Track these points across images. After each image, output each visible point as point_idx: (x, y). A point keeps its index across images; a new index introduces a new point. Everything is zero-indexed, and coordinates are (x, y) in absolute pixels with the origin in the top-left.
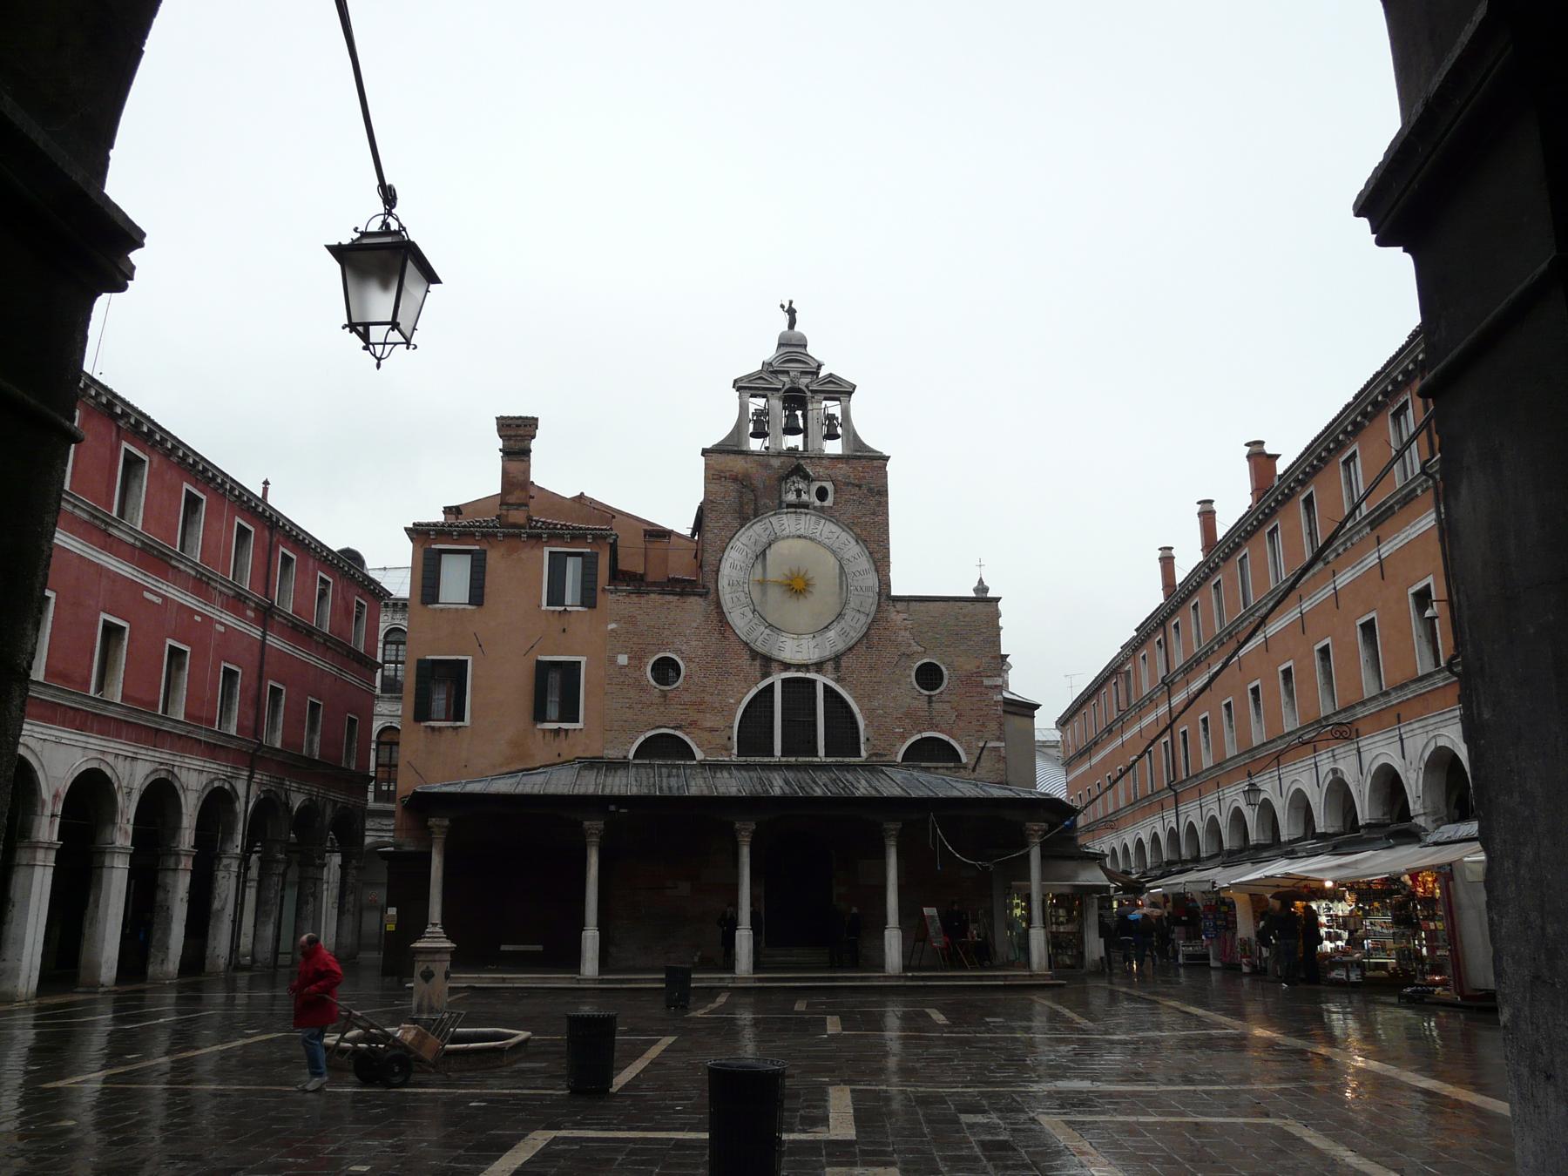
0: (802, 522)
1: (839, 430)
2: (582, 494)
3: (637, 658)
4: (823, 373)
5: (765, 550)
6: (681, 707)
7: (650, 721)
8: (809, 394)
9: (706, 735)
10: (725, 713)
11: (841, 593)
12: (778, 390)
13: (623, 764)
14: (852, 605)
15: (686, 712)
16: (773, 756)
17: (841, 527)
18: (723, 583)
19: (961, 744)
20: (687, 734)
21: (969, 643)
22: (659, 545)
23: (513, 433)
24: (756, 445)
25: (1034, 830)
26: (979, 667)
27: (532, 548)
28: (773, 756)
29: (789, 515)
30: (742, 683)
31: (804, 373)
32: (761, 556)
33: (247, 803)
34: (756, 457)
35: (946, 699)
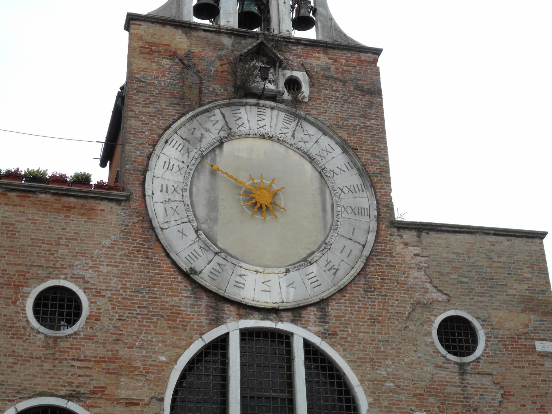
5: (213, 150)
6: (78, 364)
7: (26, 384)
10: (152, 377)
11: (324, 217)
14: (341, 230)
17: (320, 129)
26: (527, 326)
29: (248, 107)
34: (203, 34)
35: (487, 371)
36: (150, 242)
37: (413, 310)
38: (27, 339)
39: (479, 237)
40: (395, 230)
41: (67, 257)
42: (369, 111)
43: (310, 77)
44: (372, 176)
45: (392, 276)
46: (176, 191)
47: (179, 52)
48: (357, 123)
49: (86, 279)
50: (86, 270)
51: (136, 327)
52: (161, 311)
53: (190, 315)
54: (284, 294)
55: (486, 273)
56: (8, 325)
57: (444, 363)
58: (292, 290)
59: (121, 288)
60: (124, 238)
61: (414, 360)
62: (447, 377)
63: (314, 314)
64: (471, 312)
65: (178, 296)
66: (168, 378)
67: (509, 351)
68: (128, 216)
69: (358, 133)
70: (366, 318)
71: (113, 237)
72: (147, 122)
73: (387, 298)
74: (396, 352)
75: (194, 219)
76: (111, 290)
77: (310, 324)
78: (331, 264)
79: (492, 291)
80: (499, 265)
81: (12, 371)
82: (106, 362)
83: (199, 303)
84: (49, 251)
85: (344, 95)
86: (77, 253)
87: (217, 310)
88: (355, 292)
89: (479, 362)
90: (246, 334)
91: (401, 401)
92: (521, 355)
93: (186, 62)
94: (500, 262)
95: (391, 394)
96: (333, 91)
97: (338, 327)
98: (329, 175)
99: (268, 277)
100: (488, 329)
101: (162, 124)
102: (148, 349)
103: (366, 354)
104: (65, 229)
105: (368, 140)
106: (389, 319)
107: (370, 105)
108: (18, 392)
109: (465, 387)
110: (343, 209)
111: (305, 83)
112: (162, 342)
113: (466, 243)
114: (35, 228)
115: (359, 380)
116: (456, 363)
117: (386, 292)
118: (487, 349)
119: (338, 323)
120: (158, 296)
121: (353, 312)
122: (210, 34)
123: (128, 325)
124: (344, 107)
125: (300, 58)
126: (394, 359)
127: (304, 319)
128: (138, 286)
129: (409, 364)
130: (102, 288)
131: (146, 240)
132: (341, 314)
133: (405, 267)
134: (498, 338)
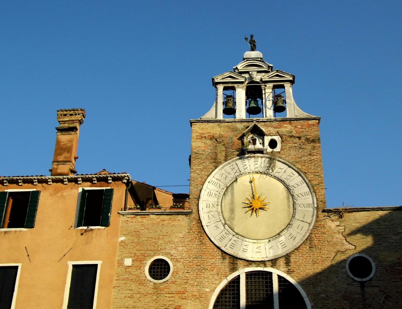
0: (259, 163)
3: (139, 260)
12: (242, 83)
15: (172, 299)
17: (287, 165)
18: (202, 205)
23: (67, 119)
30: (216, 276)
31: (258, 72)
34: (227, 124)
36: (202, 233)
37: (336, 255)
38: (146, 285)
41: (163, 245)
42: (313, 151)
43: (282, 138)
44: (314, 186)
45: (324, 238)
46: (214, 206)
47: (215, 136)
48: (306, 159)
49: (171, 254)
50: (171, 250)
51: (195, 275)
52: (207, 267)
53: (220, 268)
54: (268, 252)
55: (376, 232)
56: (137, 279)
57: (352, 282)
58: (271, 250)
59: (188, 257)
60: (189, 233)
61: (336, 282)
62: (354, 289)
63: (283, 262)
64: (368, 254)
65: (215, 259)
66: (210, 299)
67: (389, 273)
68: (191, 221)
69: (307, 164)
70: (310, 261)
71: (184, 233)
72: (199, 173)
73: (321, 250)
74: (326, 278)
75: (223, 219)
76: (183, 259)
77: (281, 267)
78: (292, 235)
79: (379, 241)
80: (384, 227)
81: (139, 301)
82: (181, 294)
83: (225, 261)
84: (155, 242)
85: (300, 145)
86: (167, 242)
87: (234, 264)
88: (304, 249)
89: (372, 281)
90: (249, 275)
92: (396, 275)
93: (218, 140)
94: (385, 225)
95: (323, 301)
96: (294, 143)
97: (295, 268)
98: (291, 188)
99: (259, 245)
100: (377, 262)
101: (207, 173)
102: (200, 286)
103: (310, 280)
104: (162, 231)
105: (312, 167)
106: (322, 261)
107: (314, 148)
109: (364, 294)
110: (299, 206)
111: (279, 142)
112: (207, 282)
113: (365, 217)
114: (148, 232)
115: (307, 294)
116: (359, 282)
117: (321, 247)
118: (377, 273)
119: (295, 265)
120: (205, 259)
121: (303, 259)
122: (230, 124)
123: (191, 275)
124: (299, 151)
125: (277, 129)
126: (325, 282)
127: (277, 265)
128: (196, 255)
129: (333, 284)
130: (179, 258)
131: (200, 232)
132: (297, 261)
133: (331, 233)
134: (382, 266)
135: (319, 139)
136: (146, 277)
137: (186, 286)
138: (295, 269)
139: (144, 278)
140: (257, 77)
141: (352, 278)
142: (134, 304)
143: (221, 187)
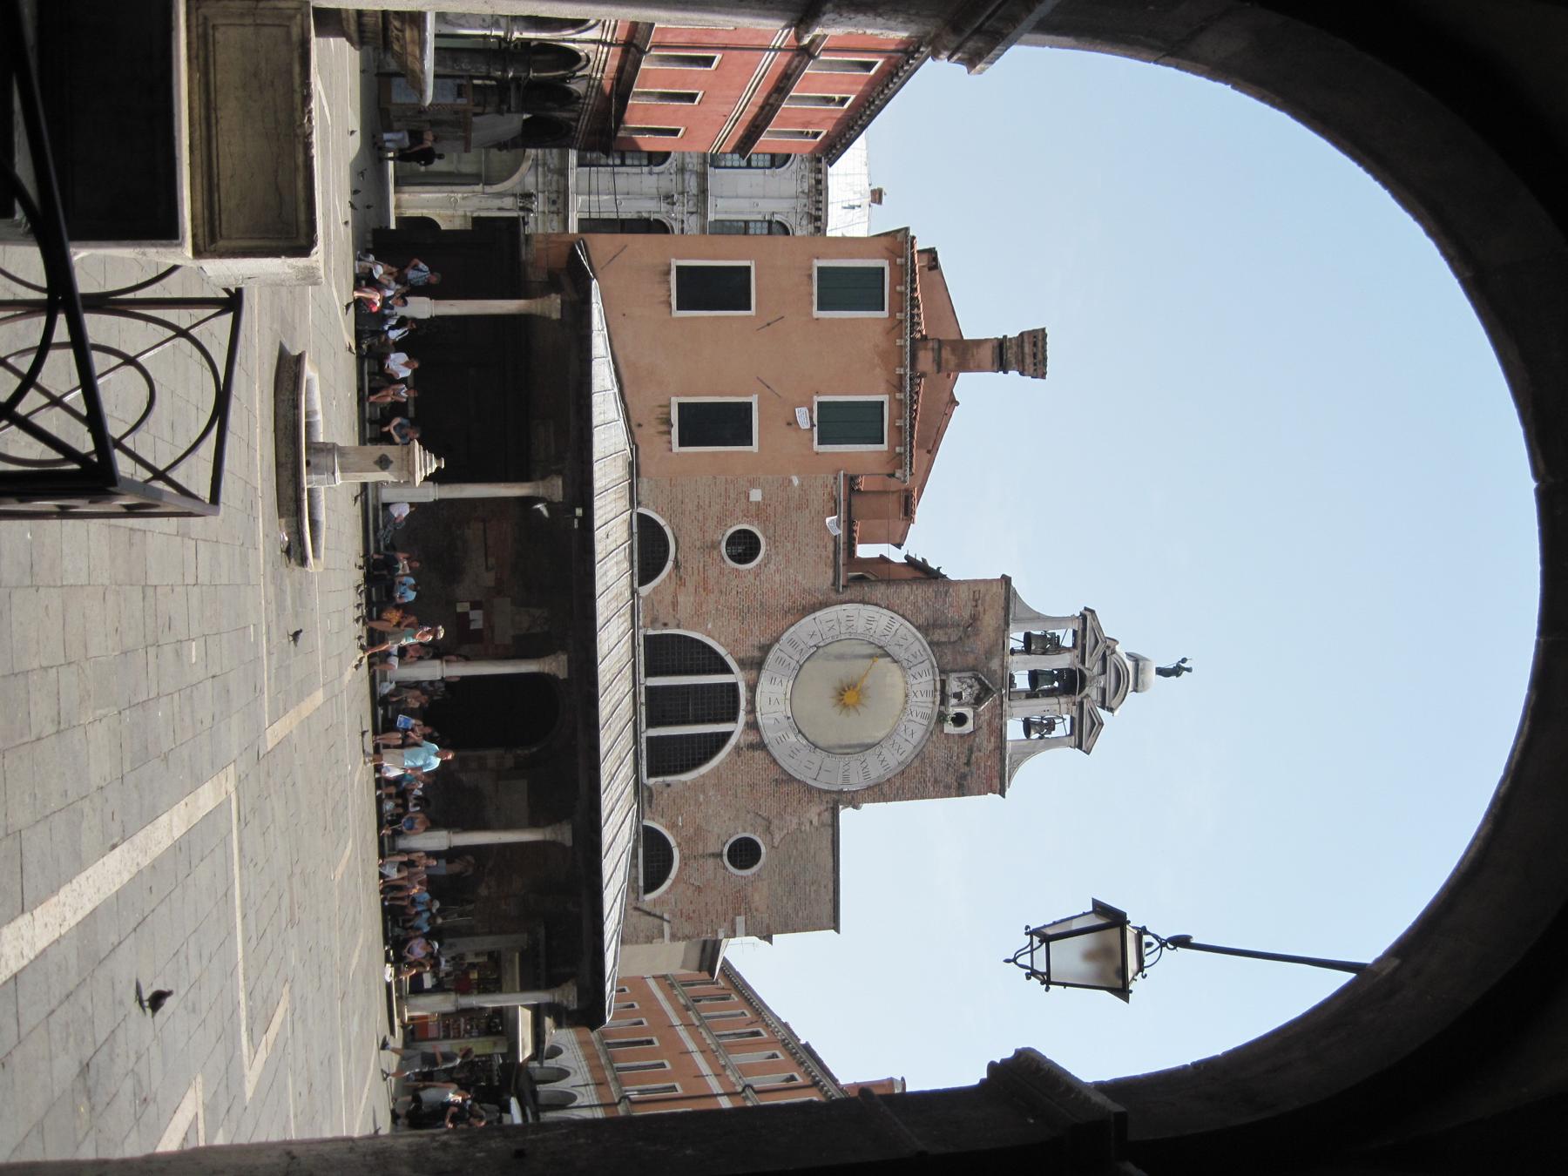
0: (924, 699)
1: (1035, 736)
2: (957, 404)
3: (759, 512)
4: (1103, 713)
5: (889, 655)
6: (701, 565)
8: (1078, 698)
9: (668, 599)
10: (695, 619)
11: (841, 747)
12: (1083, 662)
13: (634, 501)
14: (827, 760)
15: (696, 572)
16: (647, 675)
17: (919, 743)
19: (667, 892)
20: (669, 576)
21: (785, 899)
22: (892, 504)
23: (1027, 349)
24: (1016, 639)
25: (568, 997)
26: (756, 910)
27: (887, 381)
28: (647, 675)
29: (933, 682)
31: (1104, 691)
32: (883, 652)
33: (574, 41)
37: (763, 818)
39: (830, 875)
40: (832, 805)
47: (979, 623)
54: (770, 716)
71: (804, 582)
80: (808, 890)
91: (690, 806)
94: (810, 891)
99: (782, 703)
107: (948, 787)
108: (677, 526)
115: (703, 776)
116: (722, 851)
131: (804, 608)
135: (963, 795)
136: (731, 526)
137: (716, 592)
138: (743, 757)
139: (729, 525)
140: (1093, 692)
141: (727, 841)
142: (687, 513)
143: (883, 638)
